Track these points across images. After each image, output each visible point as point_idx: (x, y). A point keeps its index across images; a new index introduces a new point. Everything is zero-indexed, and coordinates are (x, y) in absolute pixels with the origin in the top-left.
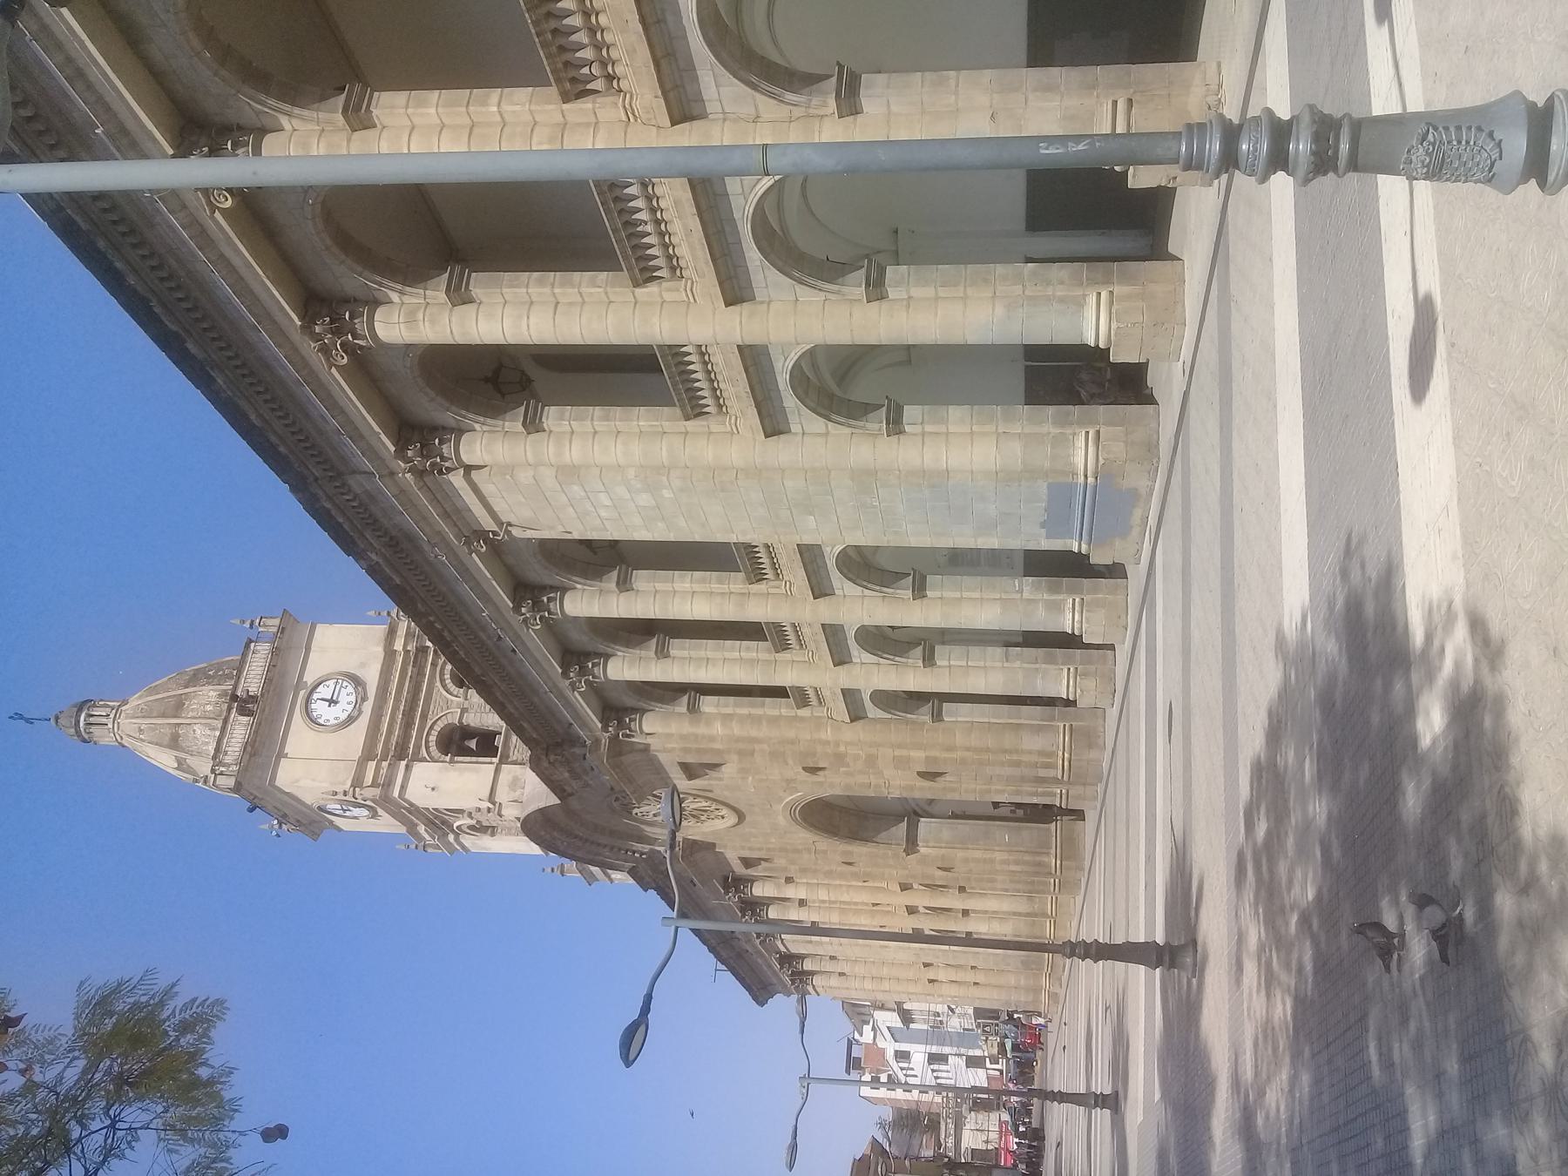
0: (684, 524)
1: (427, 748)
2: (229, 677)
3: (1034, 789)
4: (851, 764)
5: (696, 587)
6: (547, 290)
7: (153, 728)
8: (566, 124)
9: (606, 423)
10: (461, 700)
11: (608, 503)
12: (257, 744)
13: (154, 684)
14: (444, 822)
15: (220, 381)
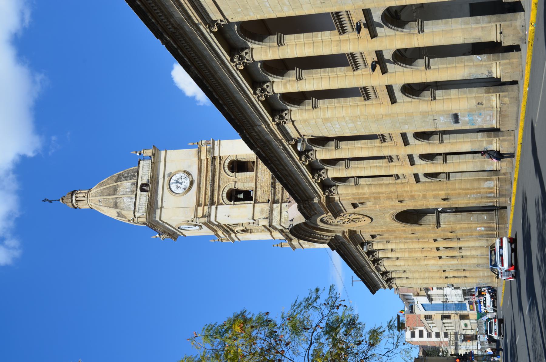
0: (363, 131)
1: (223, 199)
2: (134, 176)
3: (486, 201)
4: (417, 198)
5: (363, 146)
6: (327, 74)
7: (105, 200)
8: (340, 40)
9: (339, 104)
10: (234, 178)
11: (339, 127)
12: (152, 203)
13: (101, 182)
14: (231, 229)
15: (226, 109)
